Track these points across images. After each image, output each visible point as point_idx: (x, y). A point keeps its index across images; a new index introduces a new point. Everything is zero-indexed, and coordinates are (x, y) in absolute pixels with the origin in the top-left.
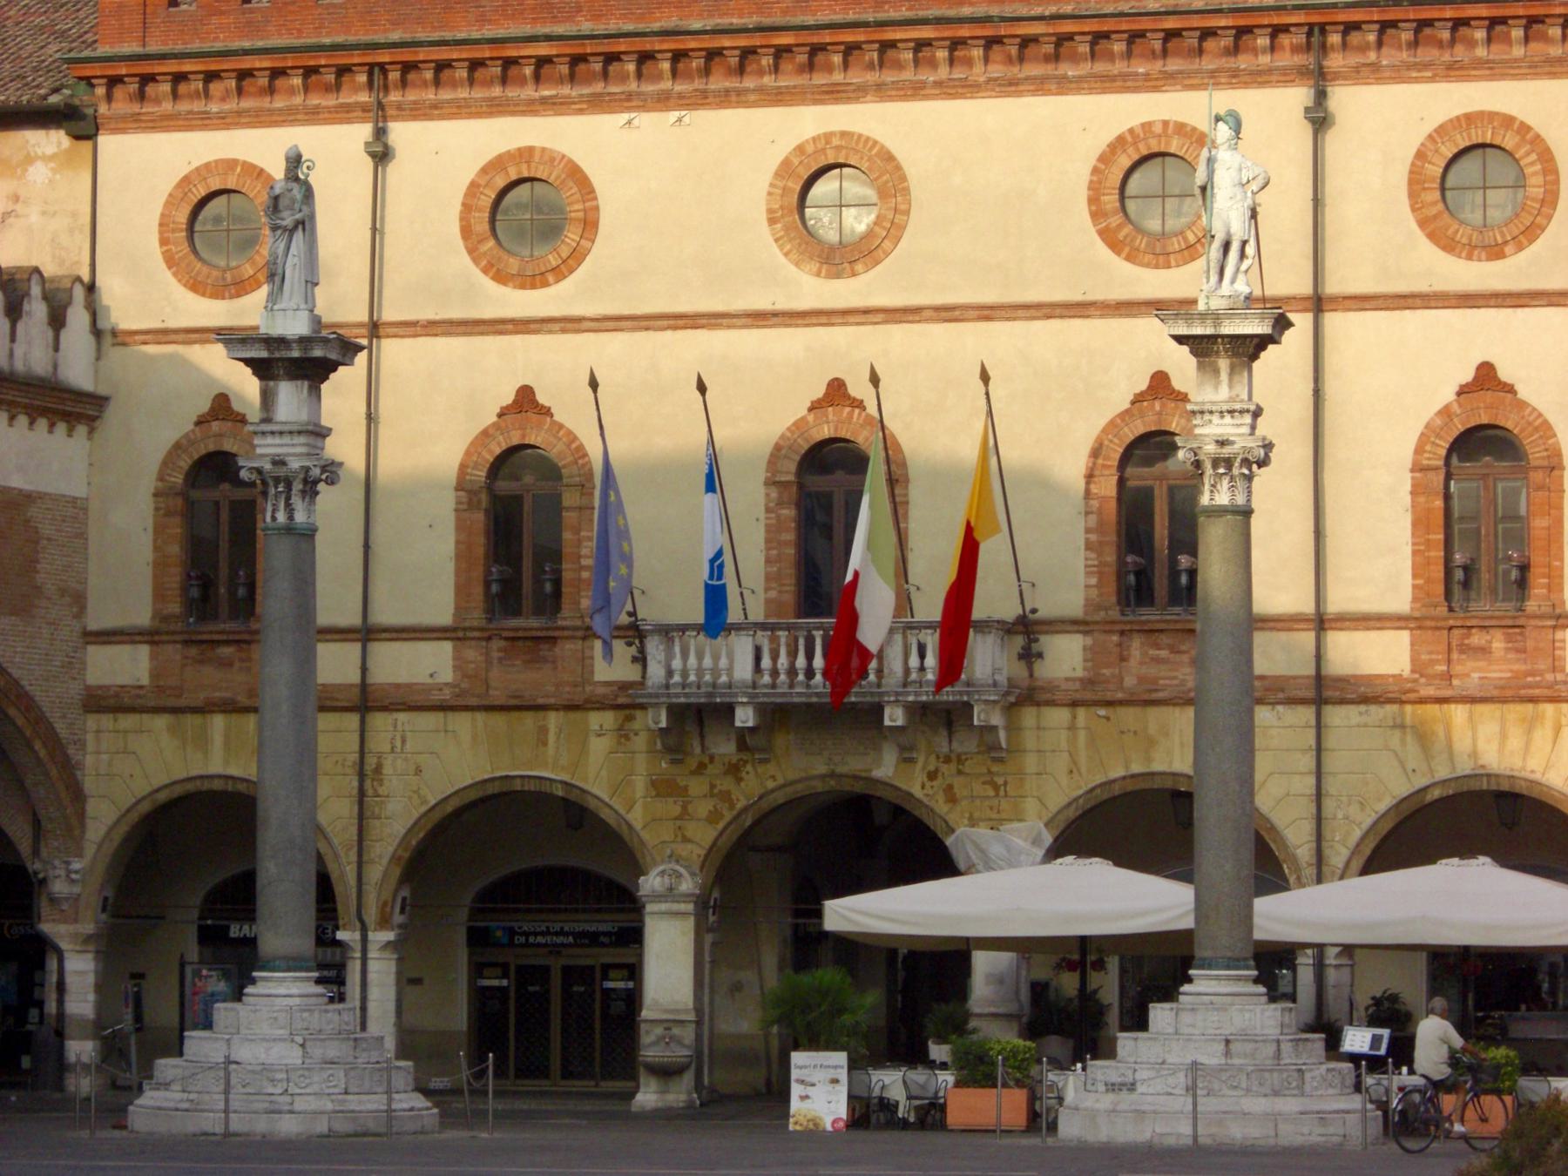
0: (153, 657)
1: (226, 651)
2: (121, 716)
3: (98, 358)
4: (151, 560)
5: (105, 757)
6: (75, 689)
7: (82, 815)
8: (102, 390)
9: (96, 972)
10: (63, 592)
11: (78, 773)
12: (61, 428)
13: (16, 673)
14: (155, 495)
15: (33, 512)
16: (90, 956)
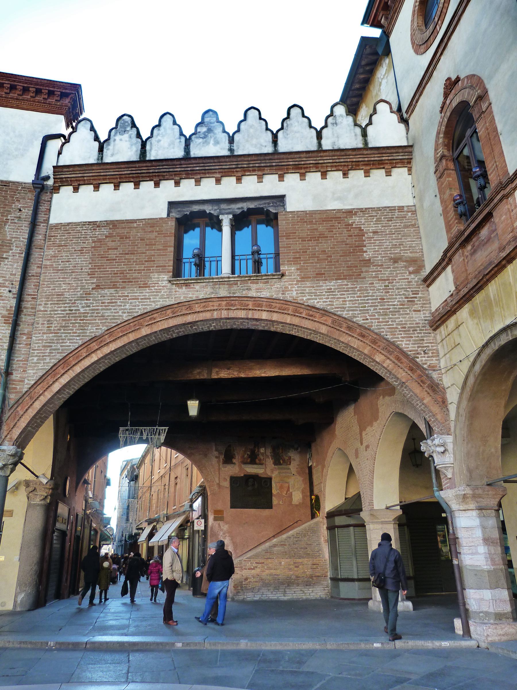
0: (453, 271)
1: (484, 232)
2: (448, 322)
3: (407, 134)
4: (441, 212)
5: (448, 356)
6: (421, 317)
7: (444, 403)
8: (410, 144)
9: (484, 528)
10: (395, 260)
11: (435, 375)
12: (378, 174)
13: (345, 314)
14: (435, 173)
15: (355, 220)
16: (475, 513)
